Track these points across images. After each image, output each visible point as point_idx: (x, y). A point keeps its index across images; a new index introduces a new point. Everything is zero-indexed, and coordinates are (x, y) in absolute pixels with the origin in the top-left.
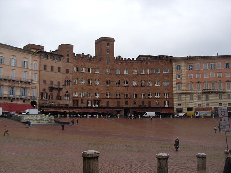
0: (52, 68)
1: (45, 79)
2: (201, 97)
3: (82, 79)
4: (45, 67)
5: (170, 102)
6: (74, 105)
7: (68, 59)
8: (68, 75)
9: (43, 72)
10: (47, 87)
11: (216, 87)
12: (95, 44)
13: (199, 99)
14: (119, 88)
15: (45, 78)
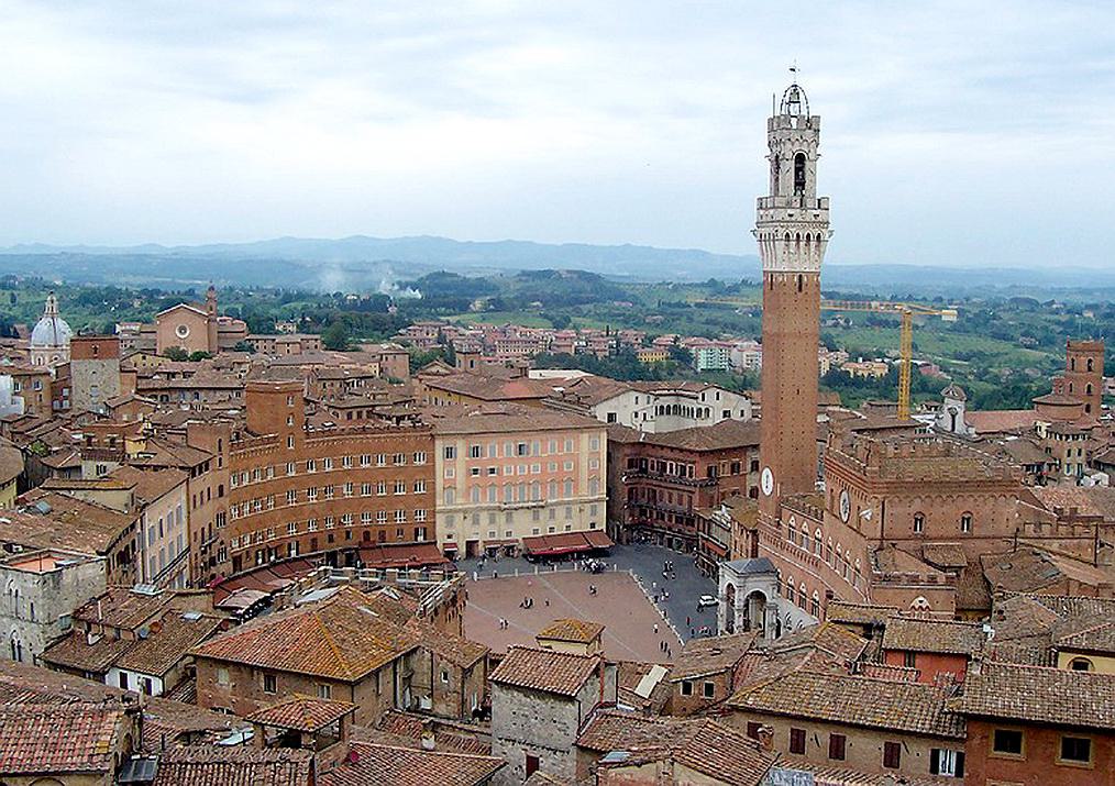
5: (429, 531)
13: (492, 521)
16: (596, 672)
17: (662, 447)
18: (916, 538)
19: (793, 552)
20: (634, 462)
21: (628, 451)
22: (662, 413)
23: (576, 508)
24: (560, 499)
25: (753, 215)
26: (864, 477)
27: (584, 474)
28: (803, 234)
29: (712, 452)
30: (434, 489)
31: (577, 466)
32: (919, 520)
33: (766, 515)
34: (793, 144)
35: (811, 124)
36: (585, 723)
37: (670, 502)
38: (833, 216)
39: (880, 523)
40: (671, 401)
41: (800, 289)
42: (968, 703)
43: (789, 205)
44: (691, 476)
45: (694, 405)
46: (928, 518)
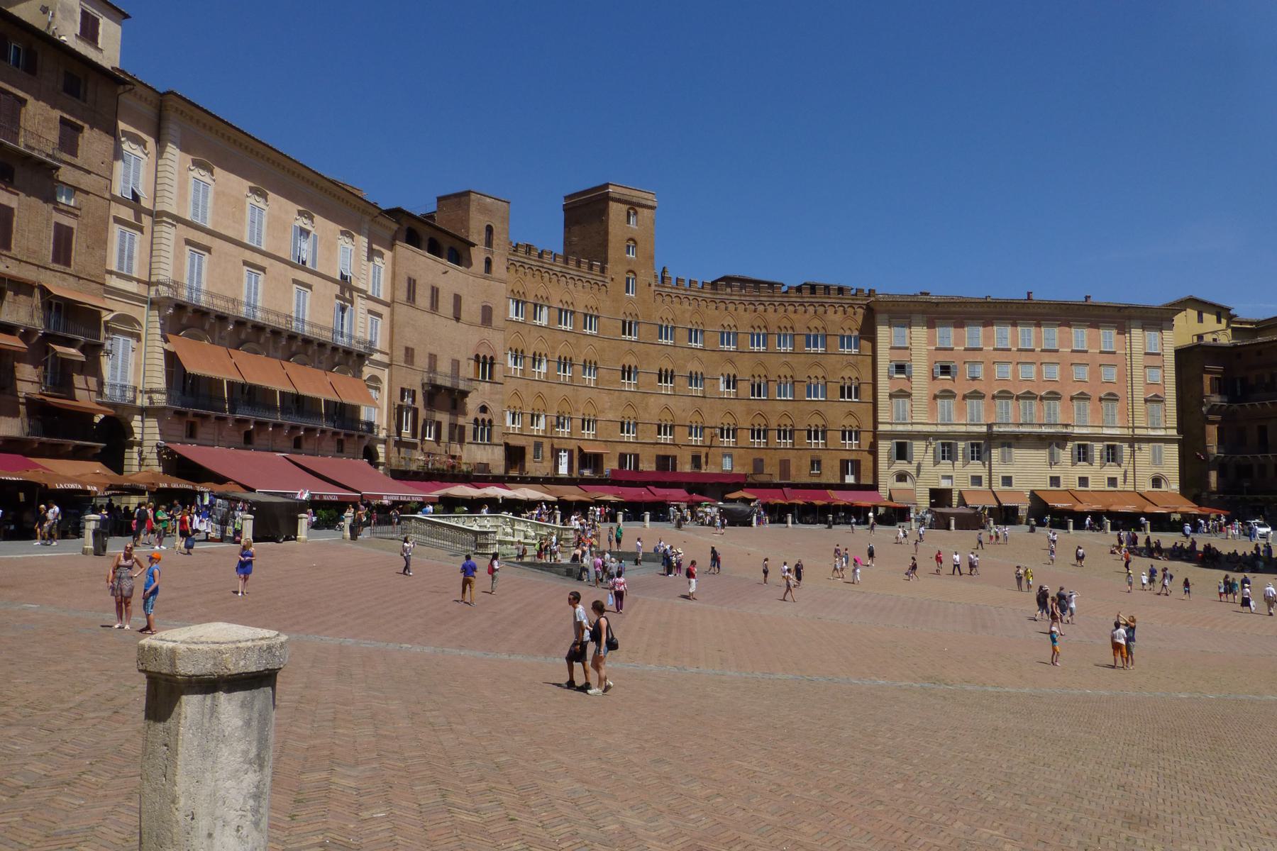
0: (435, 292)
1: (410, 345)
3: (536, 360)
4: (412, 284)
6: (506, 471)
7: (488, 262)
8: (486, 333)
9: (403, 311)
10: (415, 381)
11: (1039, 418)
12: (567, 209)
14: (672, 402)
15: (409, 338)
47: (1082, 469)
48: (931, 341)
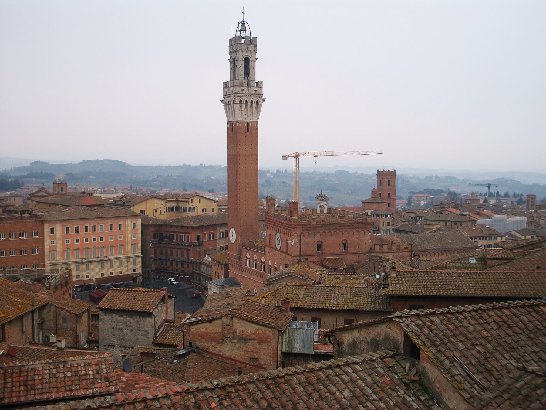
2: (80, 267)
16: (163, 300)
17: (172, 226)
18: (318, 255)
19: (249, 271)
20: (157, 235)
21: (152, 229)
22: (169, 211)
23: (124, 261)
24: (116, 256)
25: (220, 93)
26: (289, 223)
27: (129, 242)
28: (249, 100)
29: (199, 227)
30: (44, 252)
31: (125, 238)
32: (320, 245)
33: (232, 254)
34: (243, 52)
35: (252, 42)
36: (158, 331)
37: (177, 256)
38: (266, 92)
39: (299, 248)
40: (174, 205)
41: (248, 131)
42: (390, 290)
43: (241, 85)
44: (188, 241)
45: (188, 206)
46: (324, 244)
47: (112, 270)
48: (63, 232)
